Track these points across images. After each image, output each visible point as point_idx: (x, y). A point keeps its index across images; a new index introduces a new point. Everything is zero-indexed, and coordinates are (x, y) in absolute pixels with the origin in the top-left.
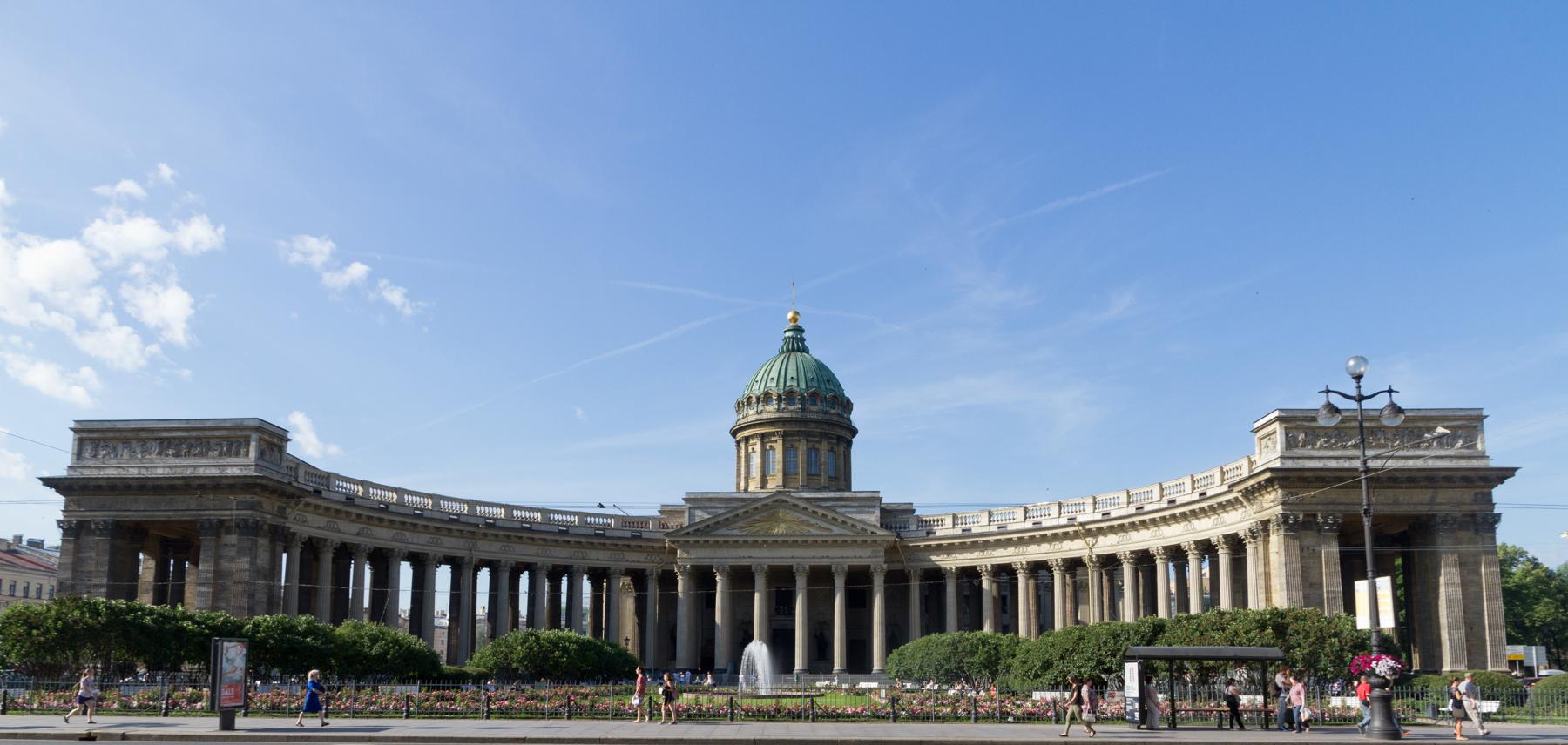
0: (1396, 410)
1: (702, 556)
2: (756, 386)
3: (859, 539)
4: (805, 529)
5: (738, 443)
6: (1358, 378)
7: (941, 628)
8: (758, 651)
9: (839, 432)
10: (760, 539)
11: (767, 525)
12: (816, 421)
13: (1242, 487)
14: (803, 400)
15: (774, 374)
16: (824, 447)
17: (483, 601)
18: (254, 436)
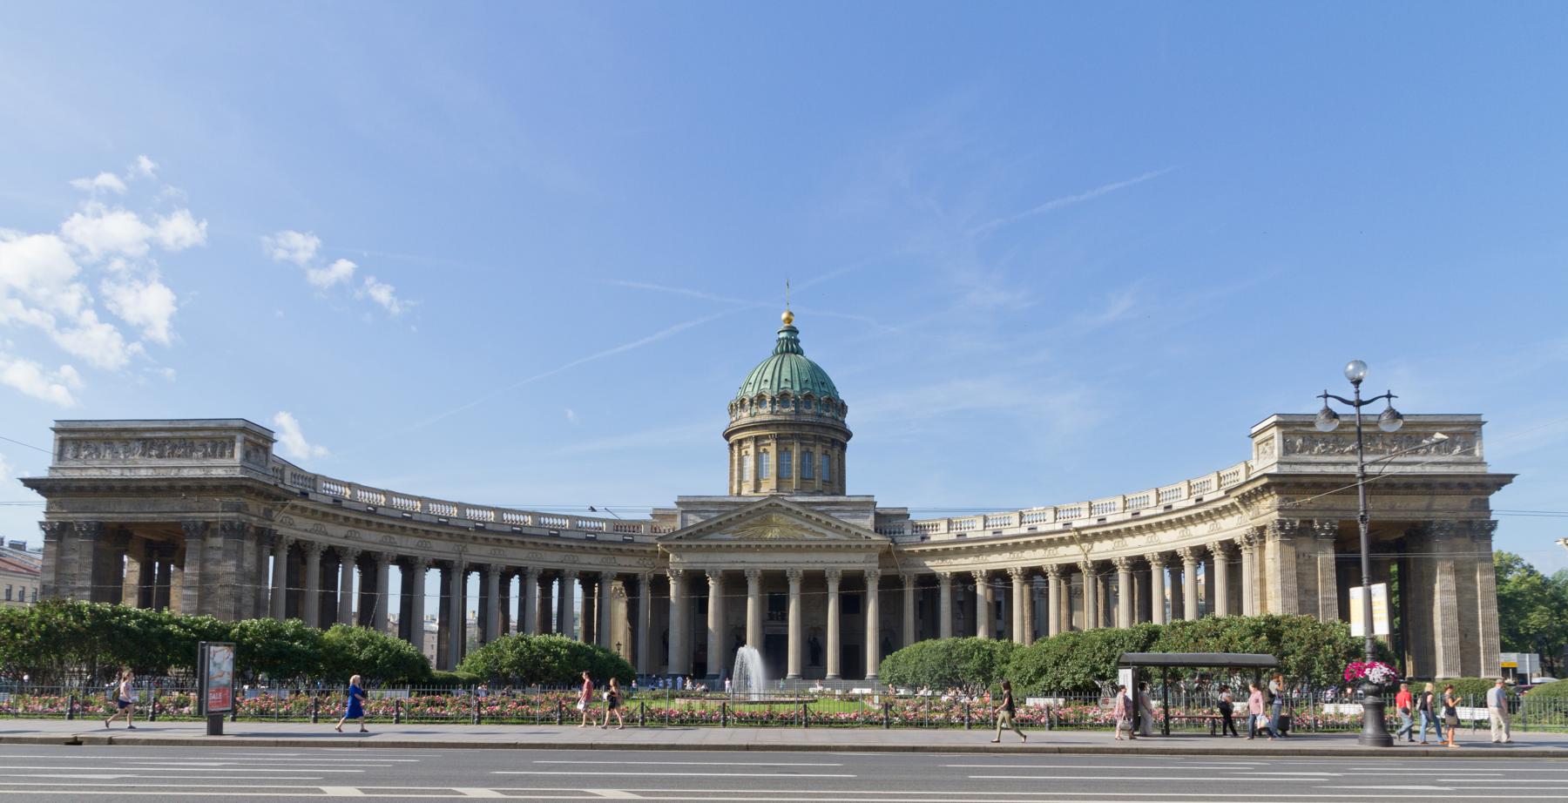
0: (1396, 416)
1: (695, 561)
2: (749, 388)
3: (853, 544)
5: (731, 446)
6: (1357, 382)
7: (935, 634)
8: (750, 656)
9: (833, 435)
10: (753, 544)
11: (760, 529)
12: (810, 424)
13: (1239, 492)
14: (797, 402)
15: (768, 376)
16: (818, 450)
17: (473, 605)
18: (239, 437)
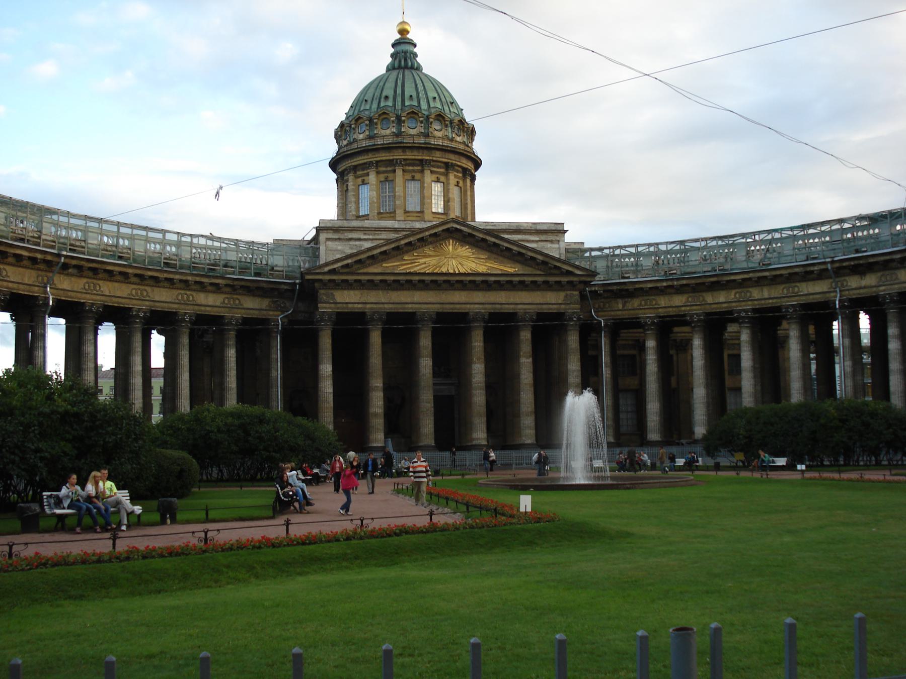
4: (482, 269)
11: (432, 261)
15: (388, 91)
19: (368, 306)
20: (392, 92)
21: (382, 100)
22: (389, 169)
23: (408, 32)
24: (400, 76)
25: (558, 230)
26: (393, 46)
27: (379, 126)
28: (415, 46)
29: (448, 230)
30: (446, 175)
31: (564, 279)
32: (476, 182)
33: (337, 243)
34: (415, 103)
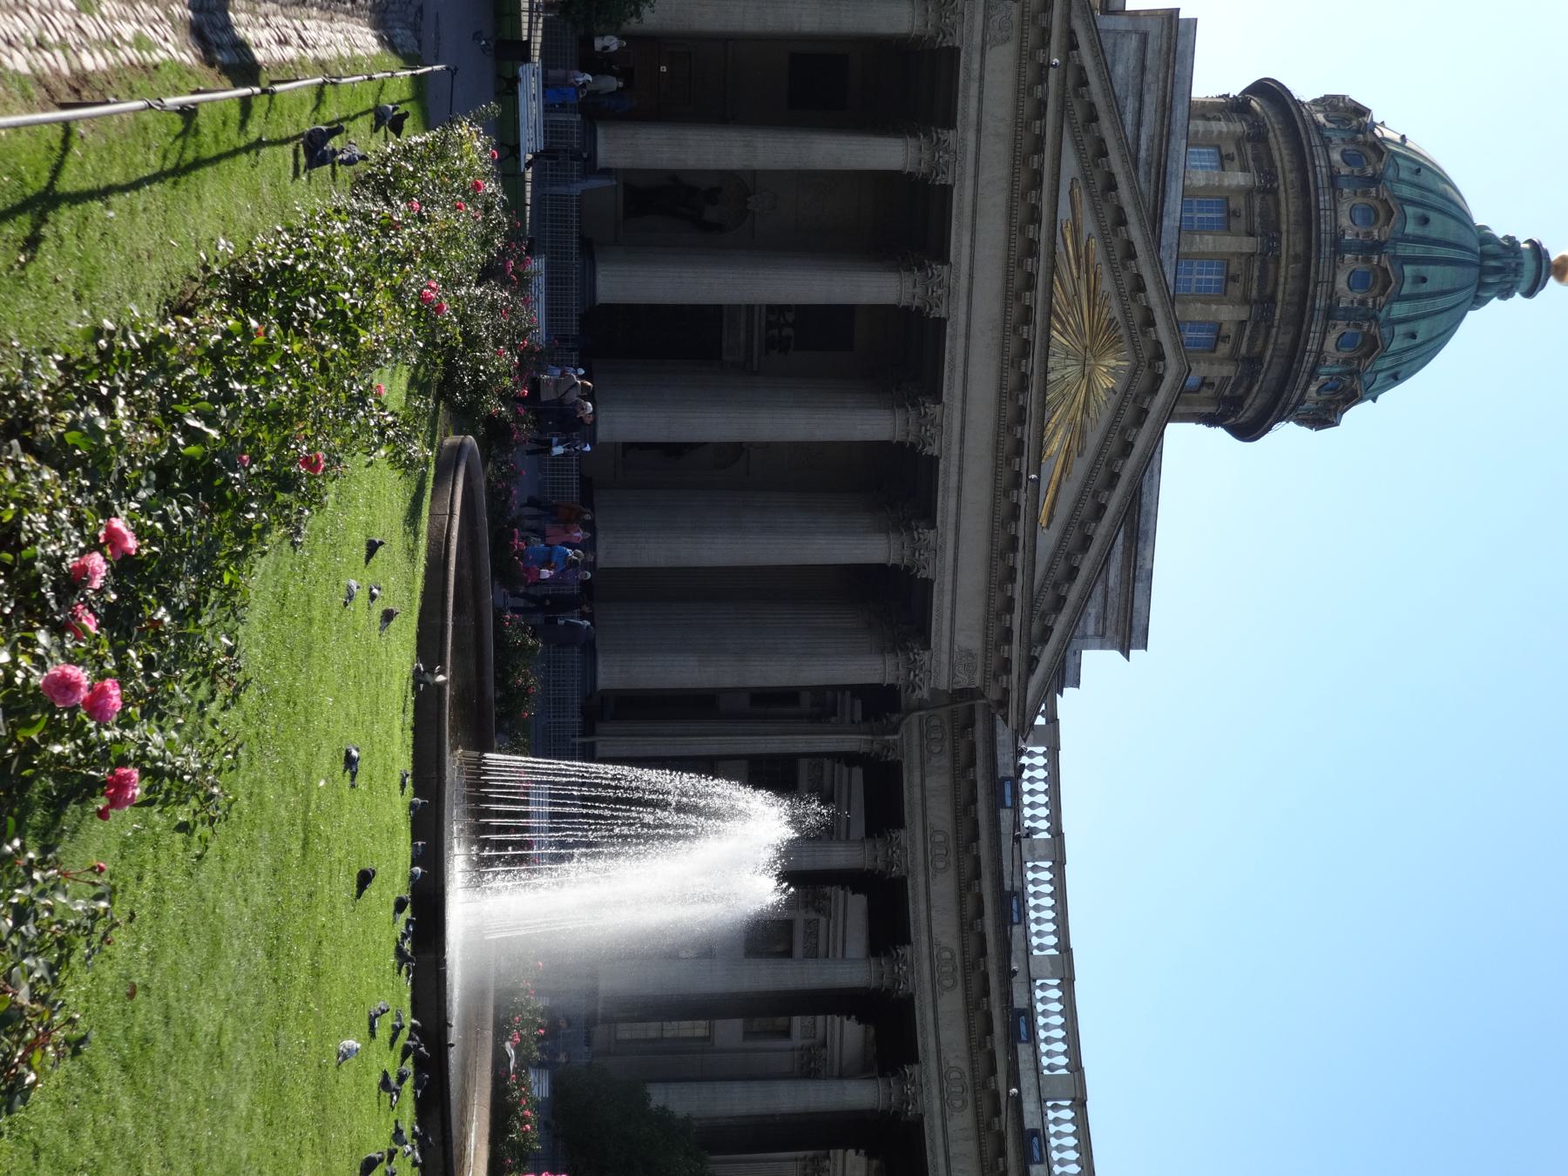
1: (989, 86)
4: (1055, 446)
9: (1254, 402)
15: (1438, 226)
16: (1221, 371)
19: (971, 137)
20: (1434, 236)
21: (1420, 211)
22: (1257, 220)
23: (1560, 278)
24: (1468, 257)
25: (1128, 633)
26: (1536, 247)
27: (1358, 200)
28: (1530, 293)
29: (1159, 356)
30: (1233, 357)
31: (1016, 651)
32: (1202, 427)
33: (1132, 63)
34: (1406, 290)
